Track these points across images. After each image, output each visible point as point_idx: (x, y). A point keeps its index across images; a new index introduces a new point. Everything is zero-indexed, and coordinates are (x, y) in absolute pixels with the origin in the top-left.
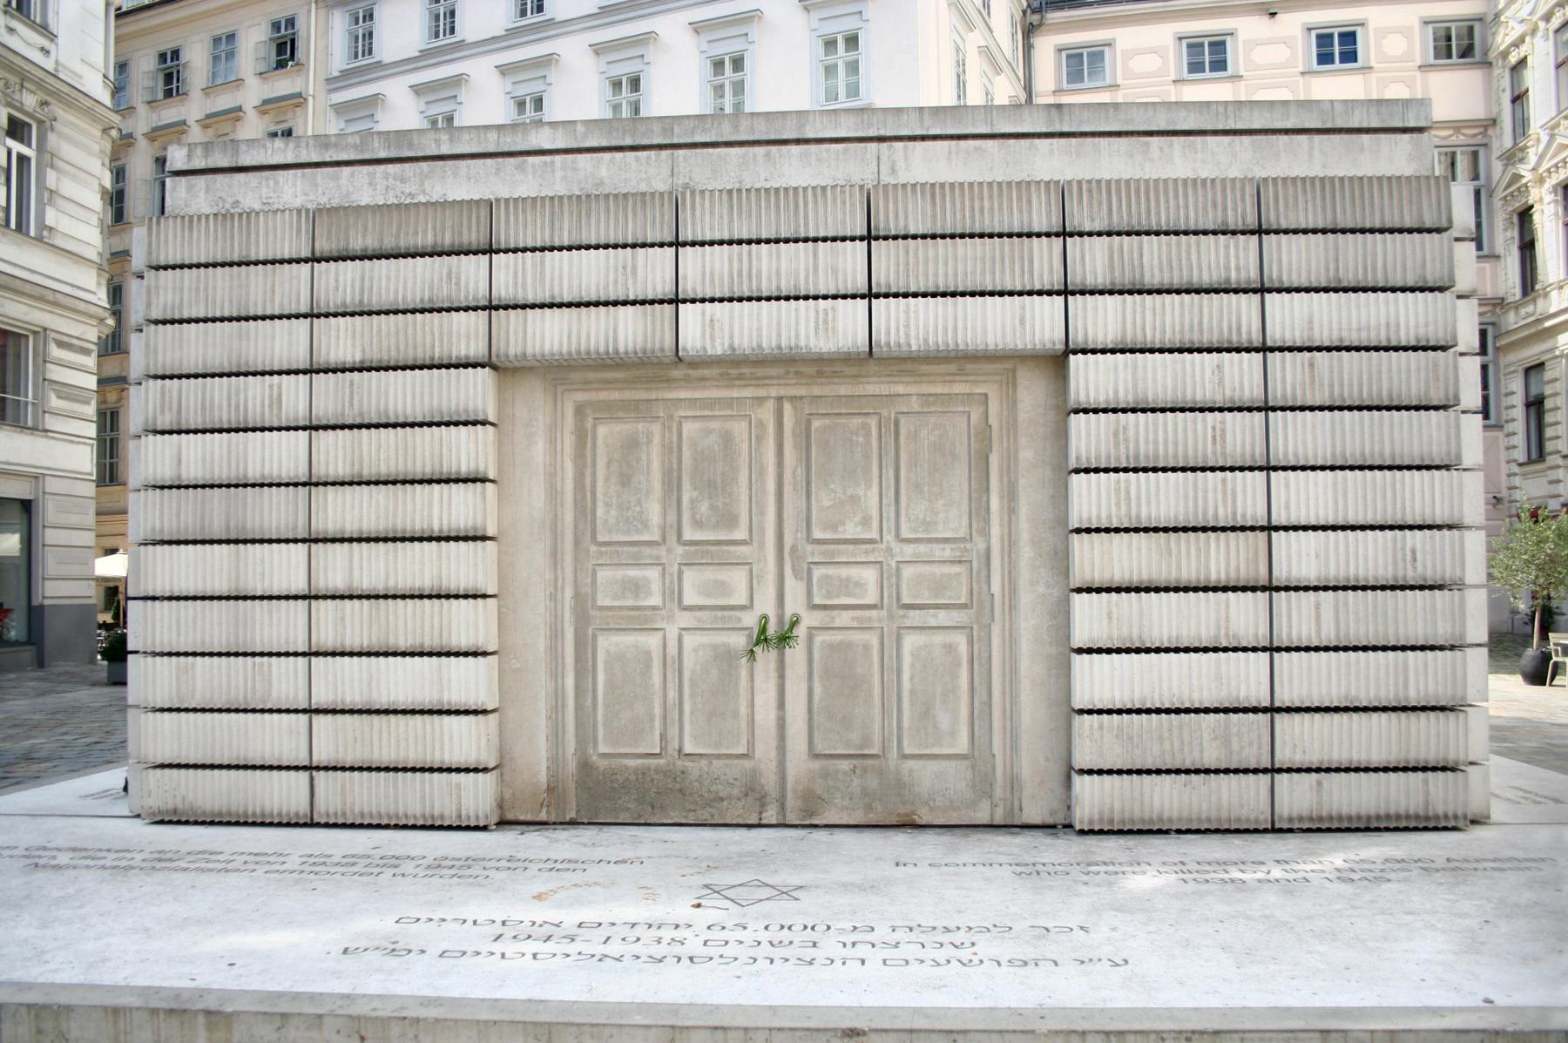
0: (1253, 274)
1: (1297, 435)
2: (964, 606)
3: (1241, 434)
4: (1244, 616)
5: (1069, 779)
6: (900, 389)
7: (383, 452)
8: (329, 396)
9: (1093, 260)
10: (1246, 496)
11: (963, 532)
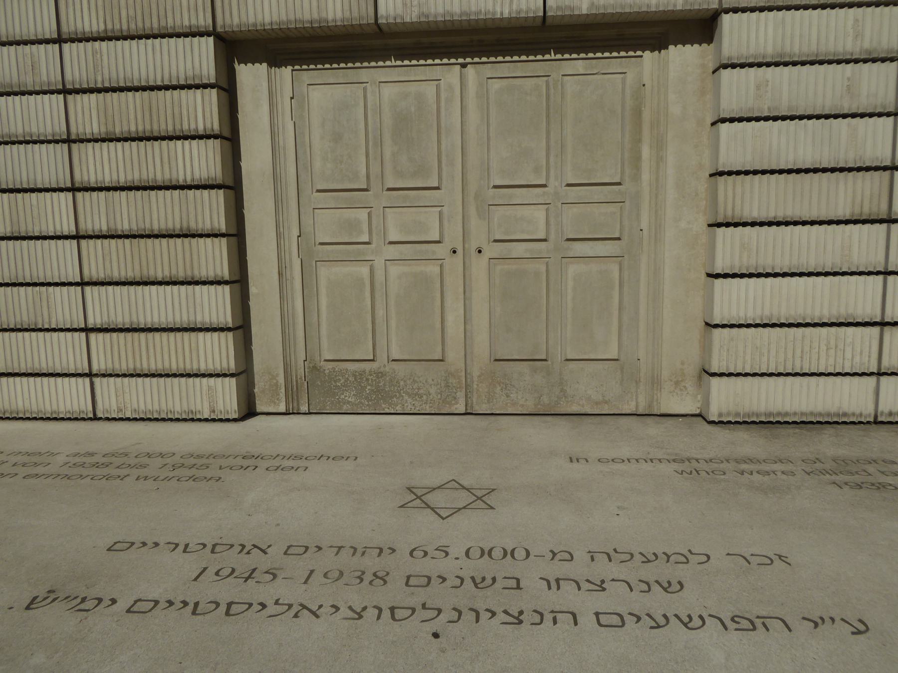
7: (130, 111)
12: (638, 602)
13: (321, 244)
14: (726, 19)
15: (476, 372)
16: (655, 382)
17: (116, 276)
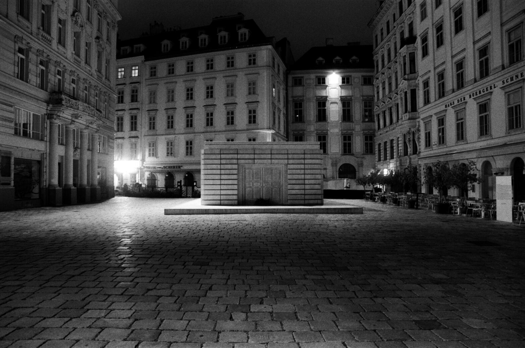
1: (307, 172)
3: (302, 172)
9: (290, 156)
10: (303, 176)
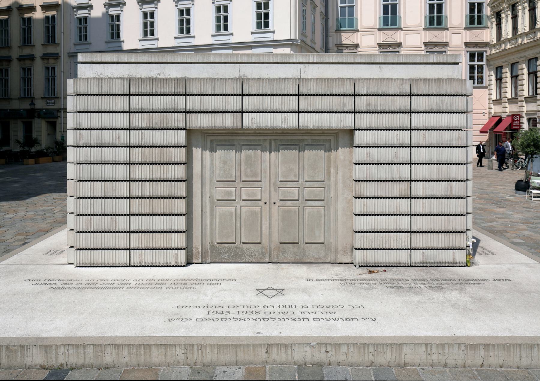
0: (409, 108)
1: (419, 154)
2: (323, 200)
3: (404, 154)
4: (403, 205)
5: (352, 250)
6: (306, 138)
7: (154, 154)
8: (136, 137)
9: (362, 103)
10: (404, 172)
11: (323, 180)
12: (324, 316)
13: (218, 200)
14: (356, 132)
15: (273, 247)
16: (336, 251)
17: (143, 212)
